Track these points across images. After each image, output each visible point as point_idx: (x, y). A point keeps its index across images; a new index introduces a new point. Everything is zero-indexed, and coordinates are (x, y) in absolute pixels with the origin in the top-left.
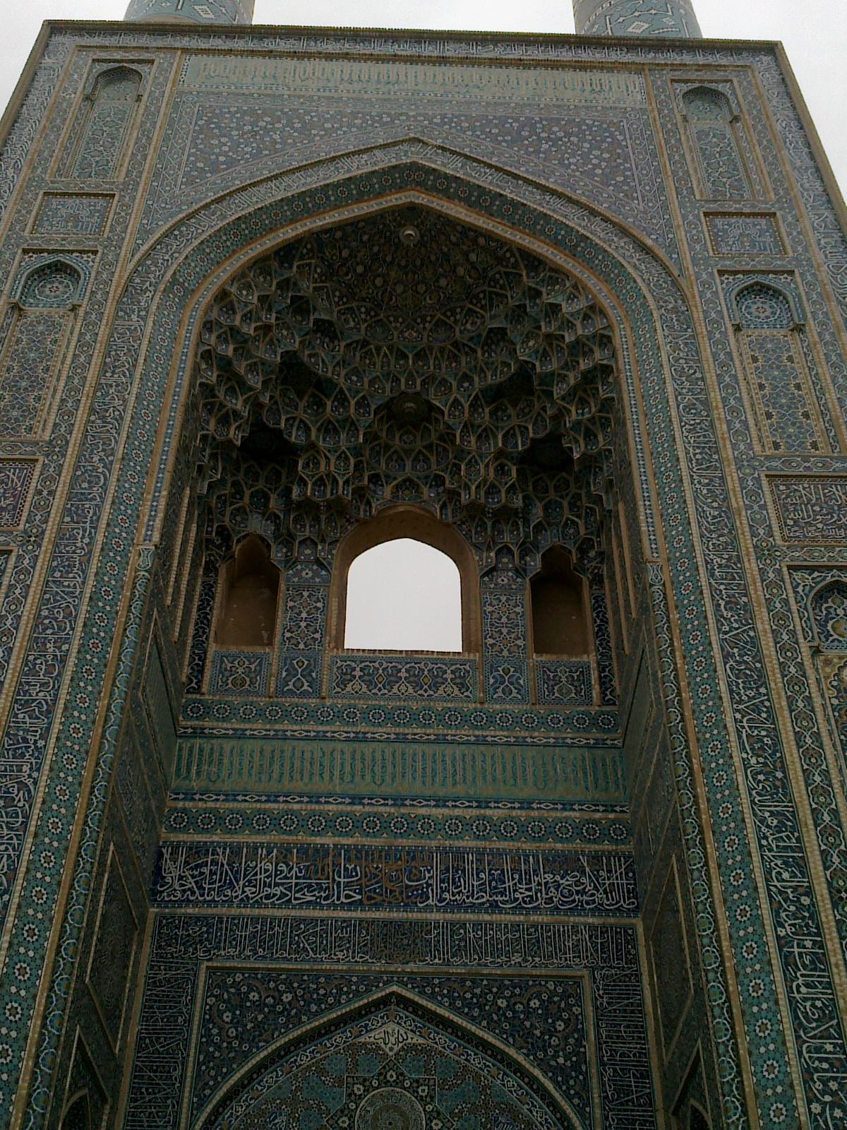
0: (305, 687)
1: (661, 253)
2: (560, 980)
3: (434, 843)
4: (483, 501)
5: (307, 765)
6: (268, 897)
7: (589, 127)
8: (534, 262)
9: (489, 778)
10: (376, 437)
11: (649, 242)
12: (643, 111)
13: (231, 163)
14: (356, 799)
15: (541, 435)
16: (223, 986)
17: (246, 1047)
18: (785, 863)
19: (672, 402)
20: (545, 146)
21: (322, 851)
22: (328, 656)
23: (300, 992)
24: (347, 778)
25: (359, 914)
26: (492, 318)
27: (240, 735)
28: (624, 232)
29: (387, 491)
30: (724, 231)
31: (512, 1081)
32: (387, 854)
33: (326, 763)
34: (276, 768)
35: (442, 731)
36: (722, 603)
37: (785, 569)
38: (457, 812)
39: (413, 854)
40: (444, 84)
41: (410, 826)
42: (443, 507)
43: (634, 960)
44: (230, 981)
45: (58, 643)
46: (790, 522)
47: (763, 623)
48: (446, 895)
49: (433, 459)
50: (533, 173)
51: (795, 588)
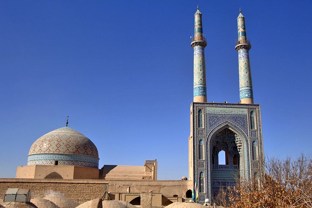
14: (221, 178)
28: (244, 134)
32: (224, 182)
39: (226, 182)
41: (225, 180)
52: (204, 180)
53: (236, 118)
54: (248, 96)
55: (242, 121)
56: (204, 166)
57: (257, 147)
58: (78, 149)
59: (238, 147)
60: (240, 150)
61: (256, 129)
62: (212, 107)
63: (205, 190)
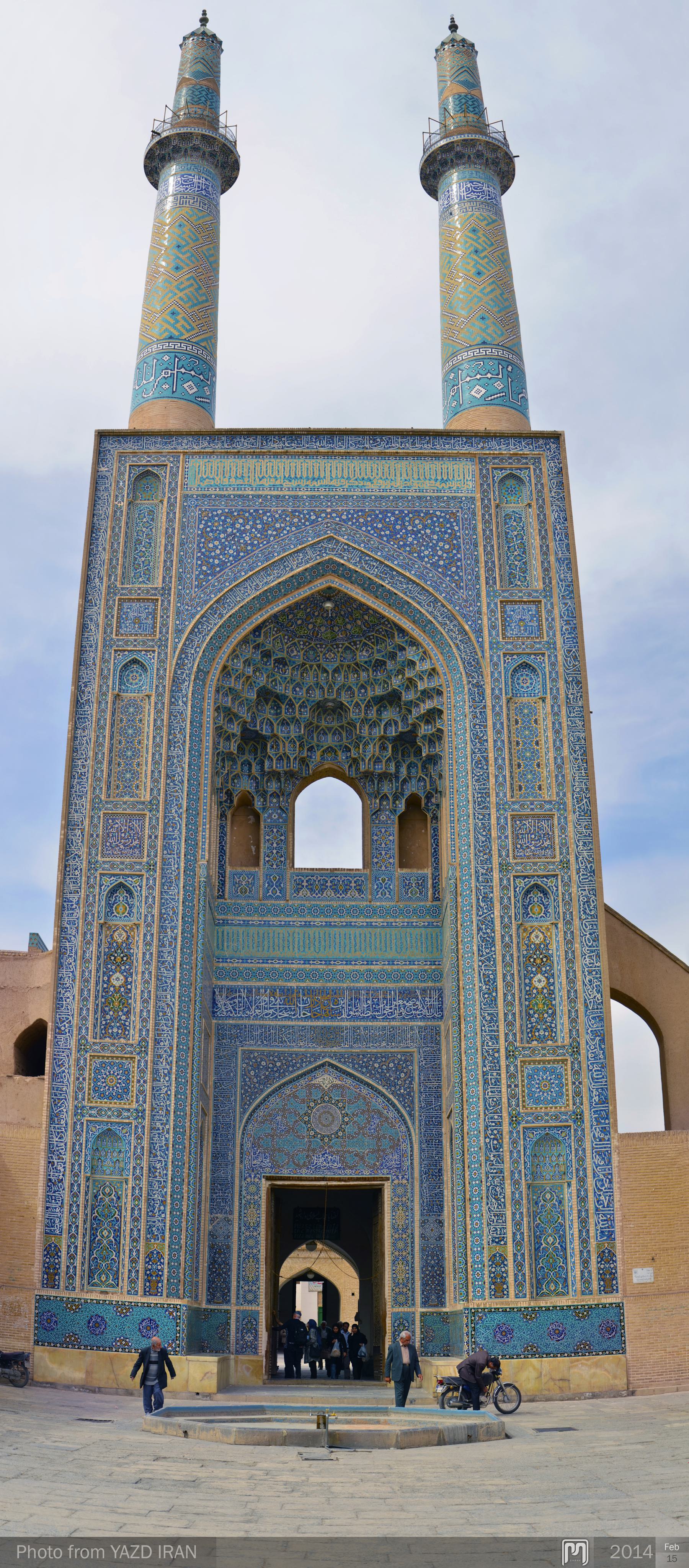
0: (278, 894)
1: (473, 637)
3: (345, 985)
4: (372, 769)
5: (281, 941)
6: (266, 1015)
7: (438, 518)
8: (401, 631)
9: (373, 947)
10: (311, 723)
14: (306, 961)
15: (406, 730)
16: (249, 1059)
17: (262, 1087)
18: (491, 1038)
19: (469, 760)
20: (410, 539)
21: (290, 990)
22: (290, 872)
23: (284, 1062)
24: (302, 949)
25: (310, 1023)
26: (379, 651)
28: (452, 618)
29: (319, 753)
32: (323, 991)
33: (291, 939)
34: (266, 943)
35: (349, 919)
36: (481, 897)
37: (512, 878)
38: (357, 967)
39: (335, 991)
40: (348, 478)
41: (332, 976)
42: (350, 766)
44: (252, 1056)
46: (519, 846)
47: (497, 913)
48: (351, 1013)
49: (344, 734)
51: (515, 888)
53: (393, 519)
55: (440, 539)
59: (424, 730)
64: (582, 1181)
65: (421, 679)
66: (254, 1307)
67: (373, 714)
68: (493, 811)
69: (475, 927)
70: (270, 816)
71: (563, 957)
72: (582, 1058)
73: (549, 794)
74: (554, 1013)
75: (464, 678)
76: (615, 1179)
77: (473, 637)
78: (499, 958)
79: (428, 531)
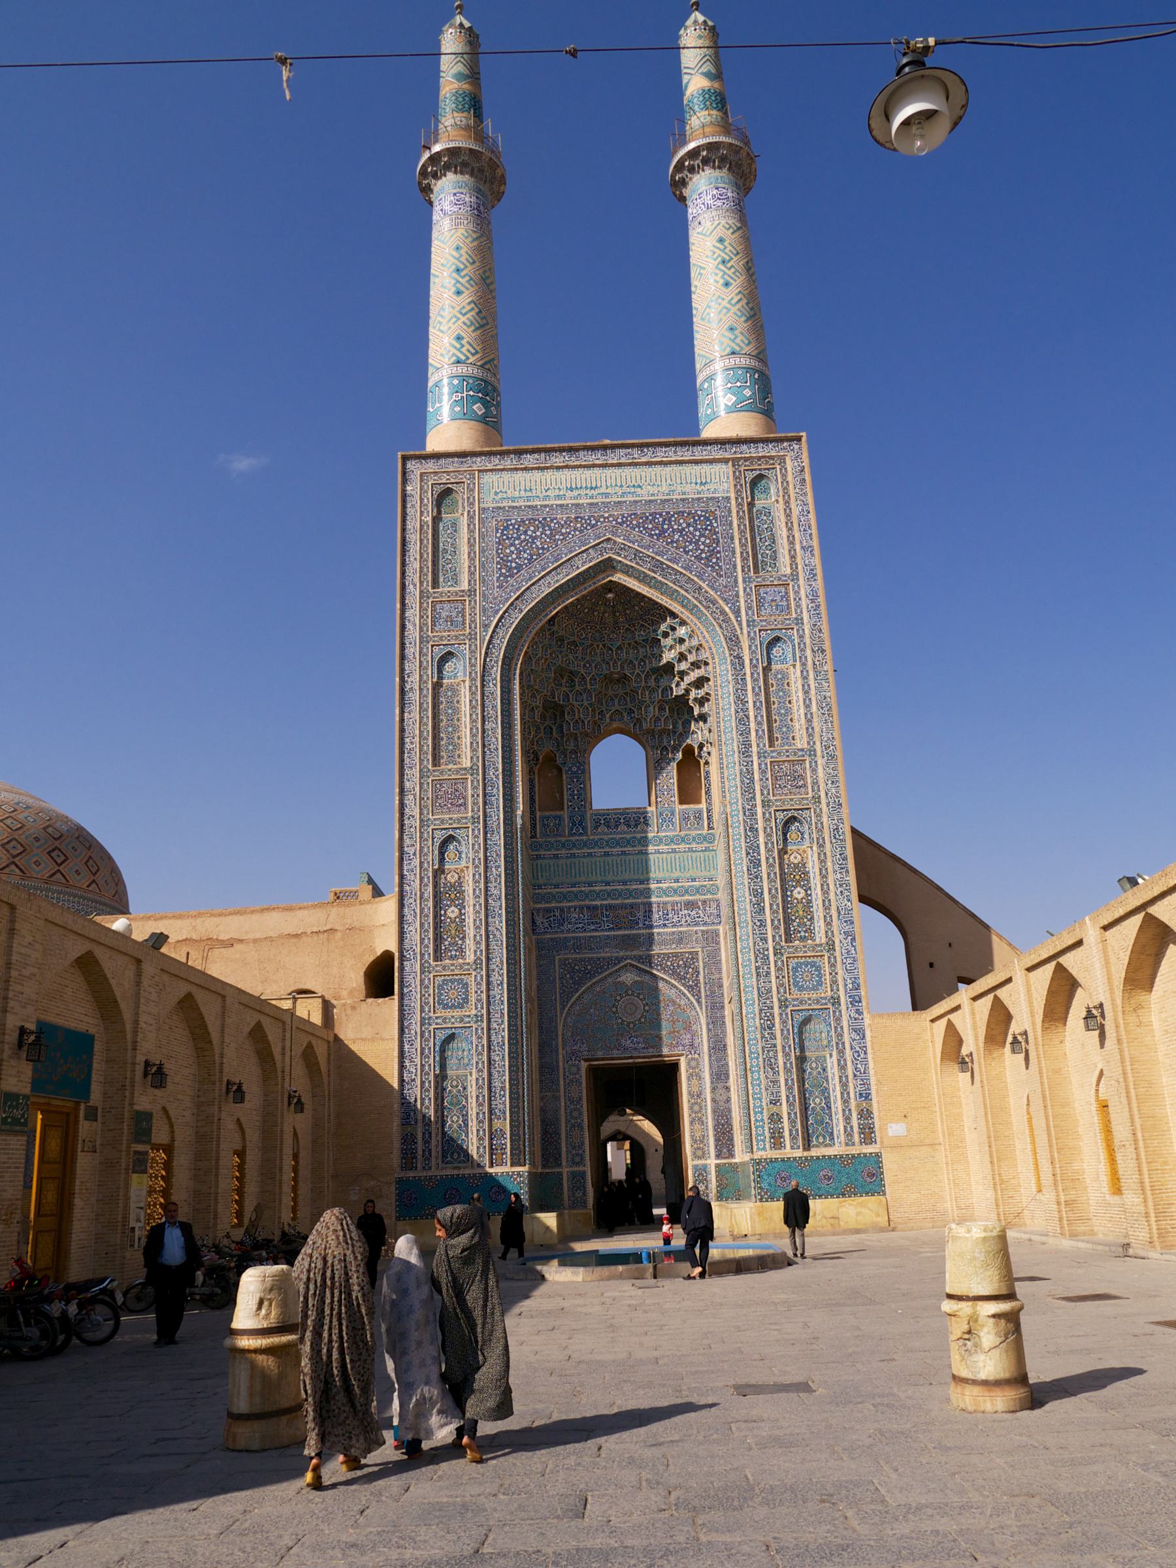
2: (690, 953)
7: (700, 517)
8: (674, 615)
11: (727, 609)
12: (728, 498)
13: (519, 568)
14: (608, 884)
21: (596, 908)
27: (556, 857)
28: (714, 602)
29: (608, 716)
30: (764, 598)
31: (674, 990)
32: (623, 907)
39: (632, 906)
43: (718, 943)
45: (498, 867)
50: (670, 560)
52: (465, 887)
53: (659, 521)
54: (735, 404)
55: (702, 535)
56: (465, 804)
57: (799, 674)
58: (14, 857)
59: (693, 694)
60: (706, 709)
61: (789, 571)
62: (520, 473)
63: (470, 943)
64: (841, 1052)
65: (690, 652)
66: (581, 1168)
67: (652, 683)
68: (755, 758)
69: (744, 852)
70: (570, 769)
71: (818, 873)
72: (838, 954)
73: (801, 743)
74: (812, 918)
75: (727, 652)
76: (869, 1051)
77: (732, 617)
78: (765, 876)
79: (691, 529)
